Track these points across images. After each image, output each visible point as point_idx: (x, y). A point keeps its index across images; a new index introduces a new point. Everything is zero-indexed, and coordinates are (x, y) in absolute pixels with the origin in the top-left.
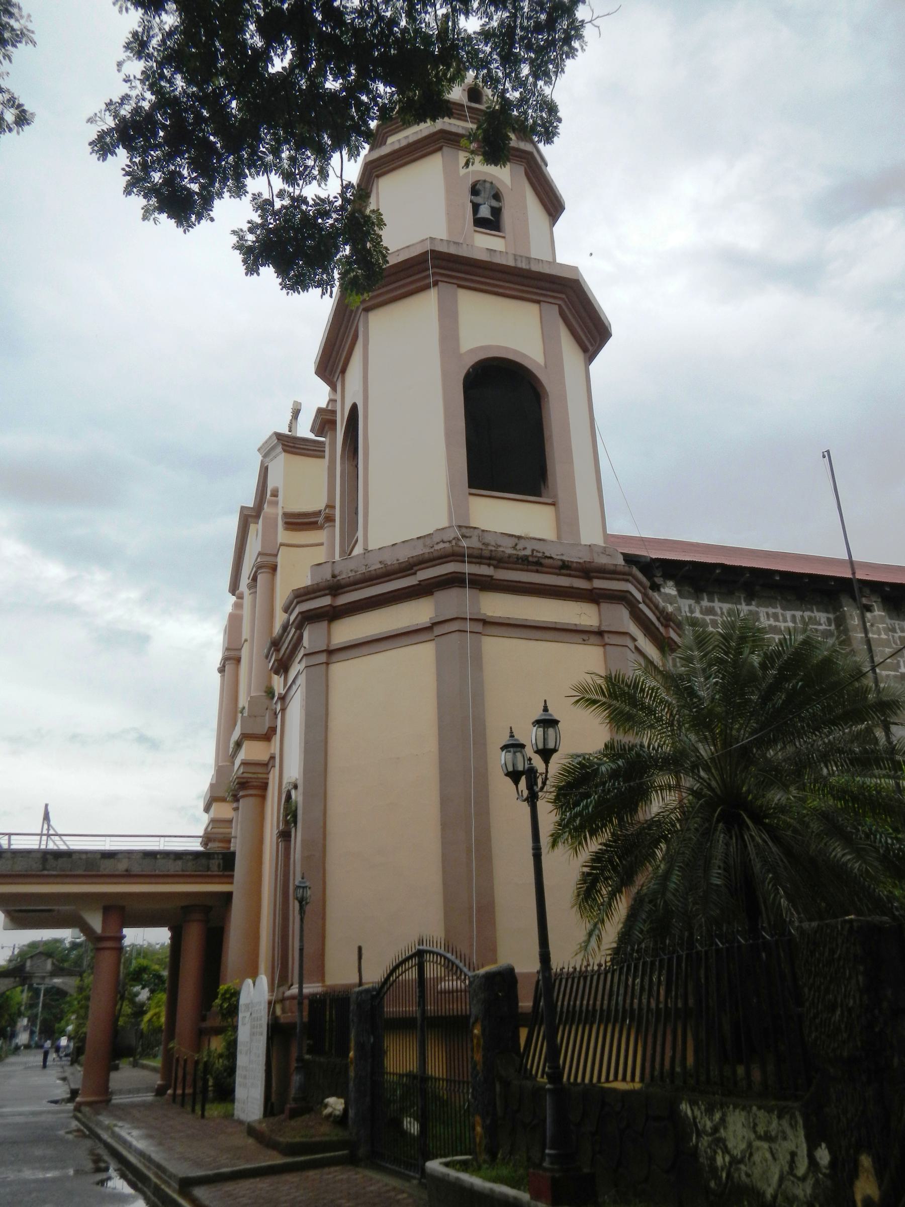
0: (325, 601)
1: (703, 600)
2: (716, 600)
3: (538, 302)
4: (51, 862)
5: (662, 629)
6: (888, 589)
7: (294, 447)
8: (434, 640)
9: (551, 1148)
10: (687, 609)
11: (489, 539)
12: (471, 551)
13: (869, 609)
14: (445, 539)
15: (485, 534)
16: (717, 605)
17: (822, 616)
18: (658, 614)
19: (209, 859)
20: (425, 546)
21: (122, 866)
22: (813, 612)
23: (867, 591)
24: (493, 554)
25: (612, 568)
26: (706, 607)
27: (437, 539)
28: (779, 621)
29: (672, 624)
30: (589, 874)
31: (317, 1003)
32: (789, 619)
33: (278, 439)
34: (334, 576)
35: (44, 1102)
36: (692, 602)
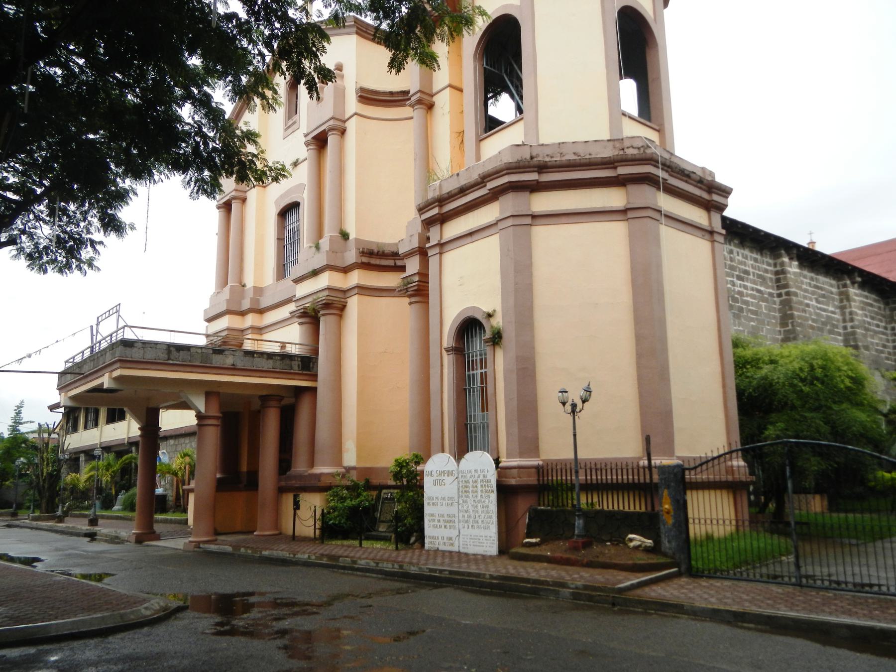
0: (534, 176)
4: (174, 353)
7: (366, 32)
8: (627, 220)
14: (635, 146)
19: (292, 360)
20: (615, 147)
27: (627, 143)
33: (355, 22)
34: (532, 158)
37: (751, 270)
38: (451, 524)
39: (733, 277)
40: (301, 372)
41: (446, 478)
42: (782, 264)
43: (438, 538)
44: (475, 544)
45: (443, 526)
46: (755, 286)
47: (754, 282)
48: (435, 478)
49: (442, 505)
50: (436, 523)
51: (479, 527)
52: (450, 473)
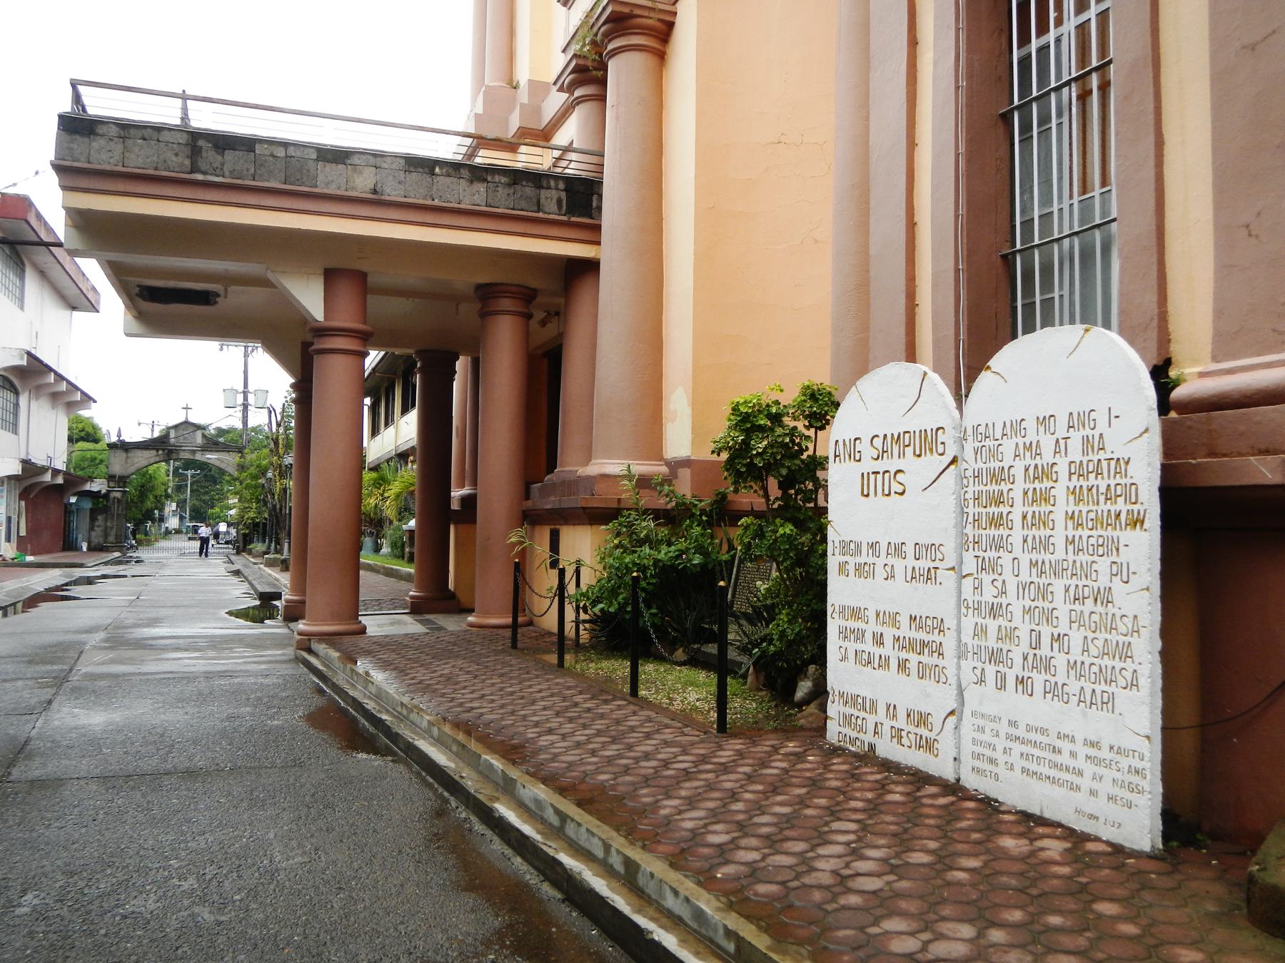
19: (540, 187)
35: (223, 613)
38: (925, 659)
40: (565, 218)
41: (908, 462)
43: (874, 708)
44: (1033, 767)
45: (894, 664)
48: (868, 465)
49: (890, 576)
50: (868, 646)
51: (1054, 691)
52: (927, 442)
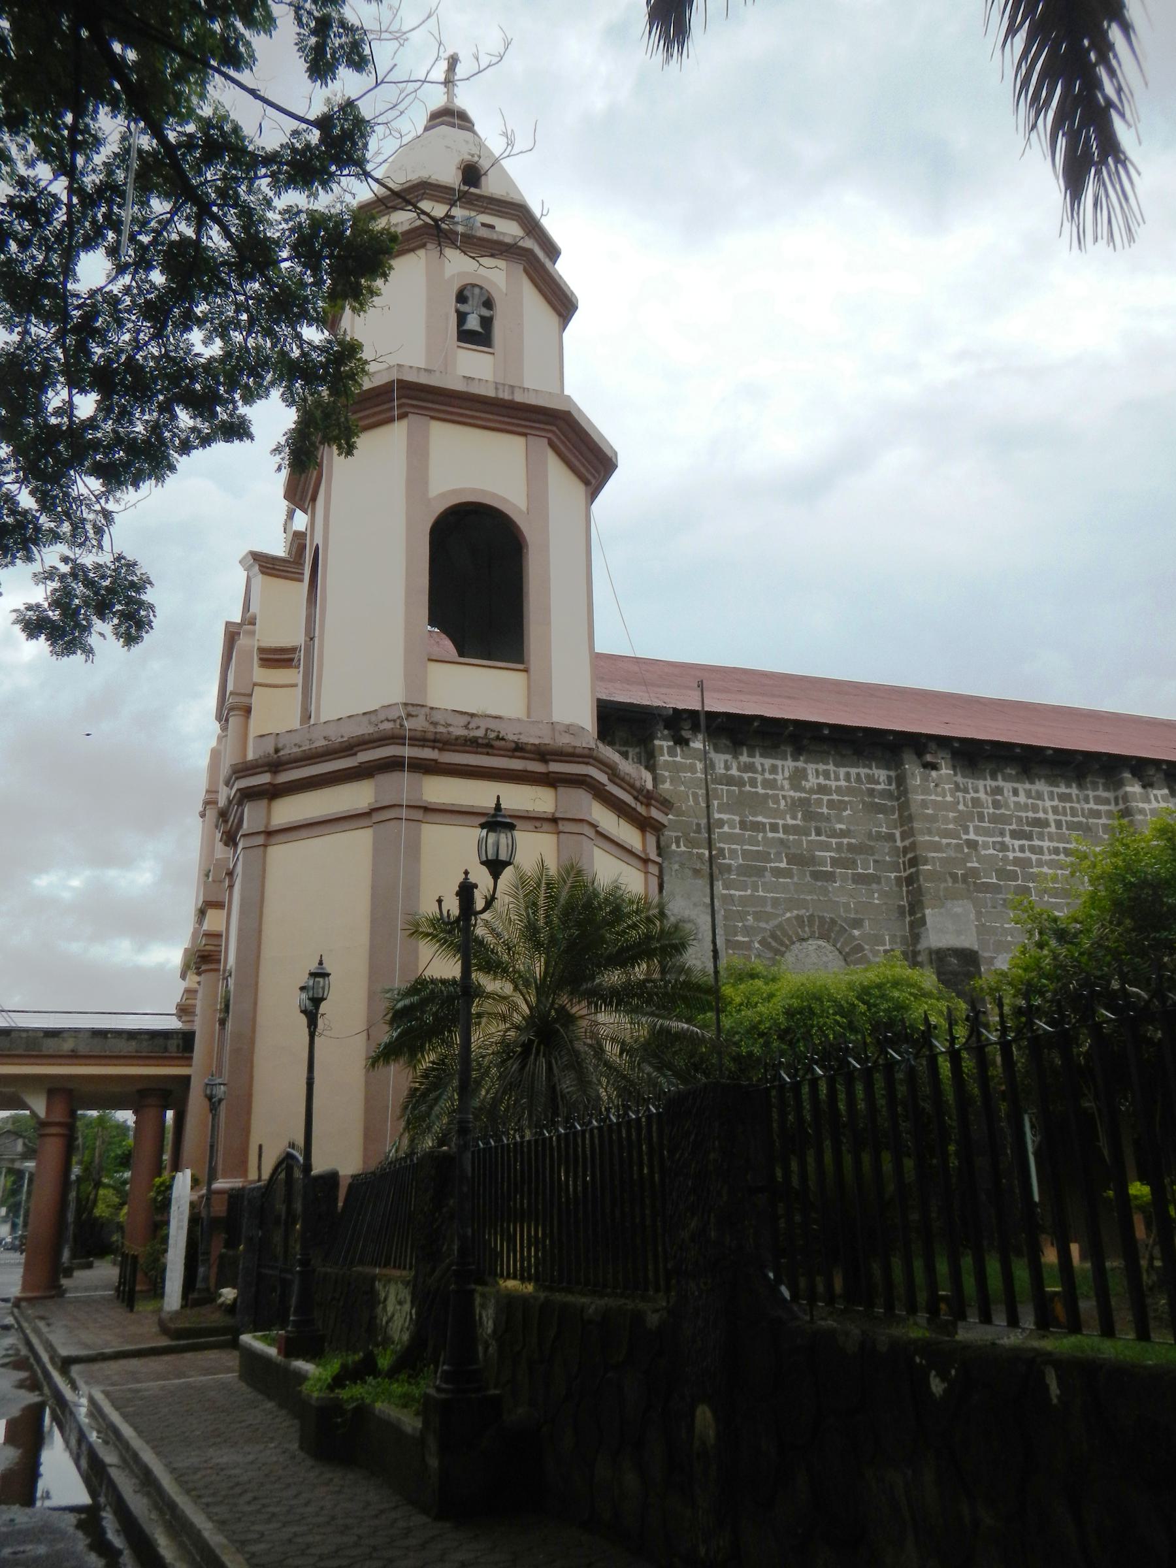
1: (742, 754)
2: (758, 754)
3: (525, 435)
5: (641, 809)
6: (956, 745)
7: (274, 569)
9: (294, 1316)
10: (722, 766)
11: (437, 717)
12: (413, 734)
13: (934, 767)
14: (390, 718)
15: (434, 712)
16: (758, 761)
17: (881, 774)
18: (635, 794)
20: (370, 723)
21: (68, 1045)
22: (871, 768)
23: (933, 746)
24: (438, 736)
25: (571, 750)
26: (745, 763)
27: (382, 716)
28: (830, 780)
29: (653, 802)
30: (416, 1089)
31: (235, 1197)
32: (842, 777)
34: (277, 751)
36: (728, 757)
37: (1051, 817)
39: (1002, 834)
40: (180, 1055)
42: (1126, 798)
46: (1061, 845)
47: (1062, 838)
